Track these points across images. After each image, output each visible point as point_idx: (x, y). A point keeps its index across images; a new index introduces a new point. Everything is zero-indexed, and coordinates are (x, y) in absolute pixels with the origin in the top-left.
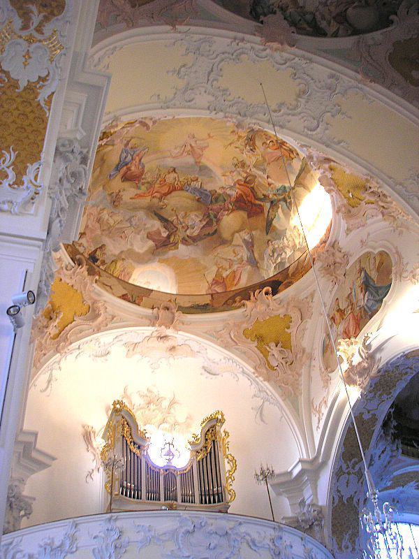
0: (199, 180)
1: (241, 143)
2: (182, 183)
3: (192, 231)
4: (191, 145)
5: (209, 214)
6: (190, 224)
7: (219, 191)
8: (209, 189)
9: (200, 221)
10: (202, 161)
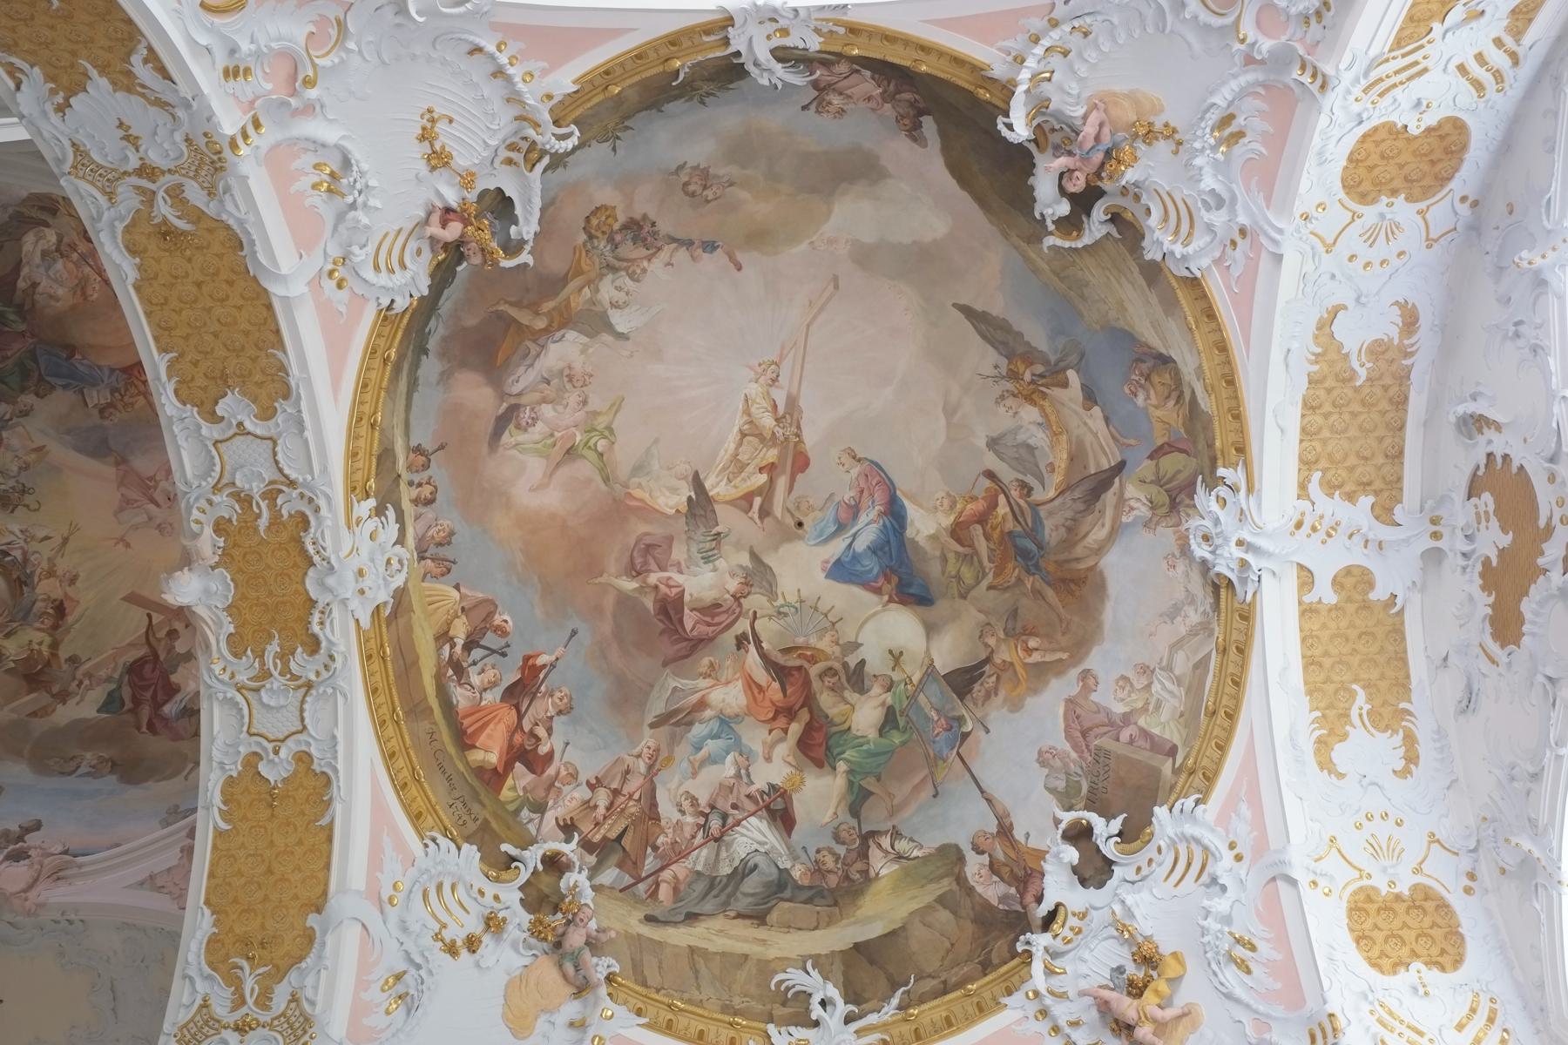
0: (96, 412)
1: (42, 555)
2: (133, 390)
3: (42, 245)
4: (158, 505)
5: (24, 320)
6: (59, 265)
7: (28, 399)
8: (59, 392)
9: (35, 285)
10: (113, 470)
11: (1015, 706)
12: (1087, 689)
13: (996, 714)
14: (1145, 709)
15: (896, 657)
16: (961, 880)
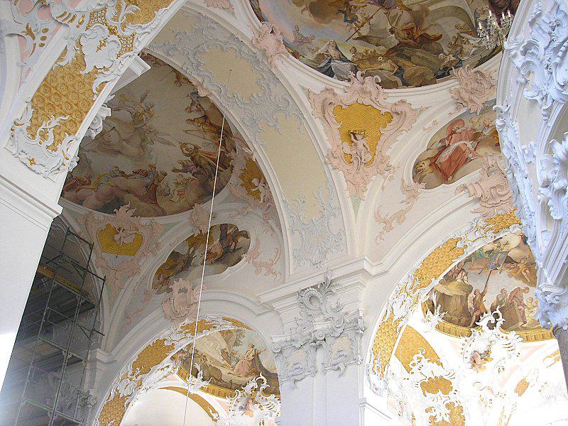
11: (510, 275)
12: (524, 291)
13: (505, 272)
14: (529, 309)
15: (507, 243)
16: (467, 296)
